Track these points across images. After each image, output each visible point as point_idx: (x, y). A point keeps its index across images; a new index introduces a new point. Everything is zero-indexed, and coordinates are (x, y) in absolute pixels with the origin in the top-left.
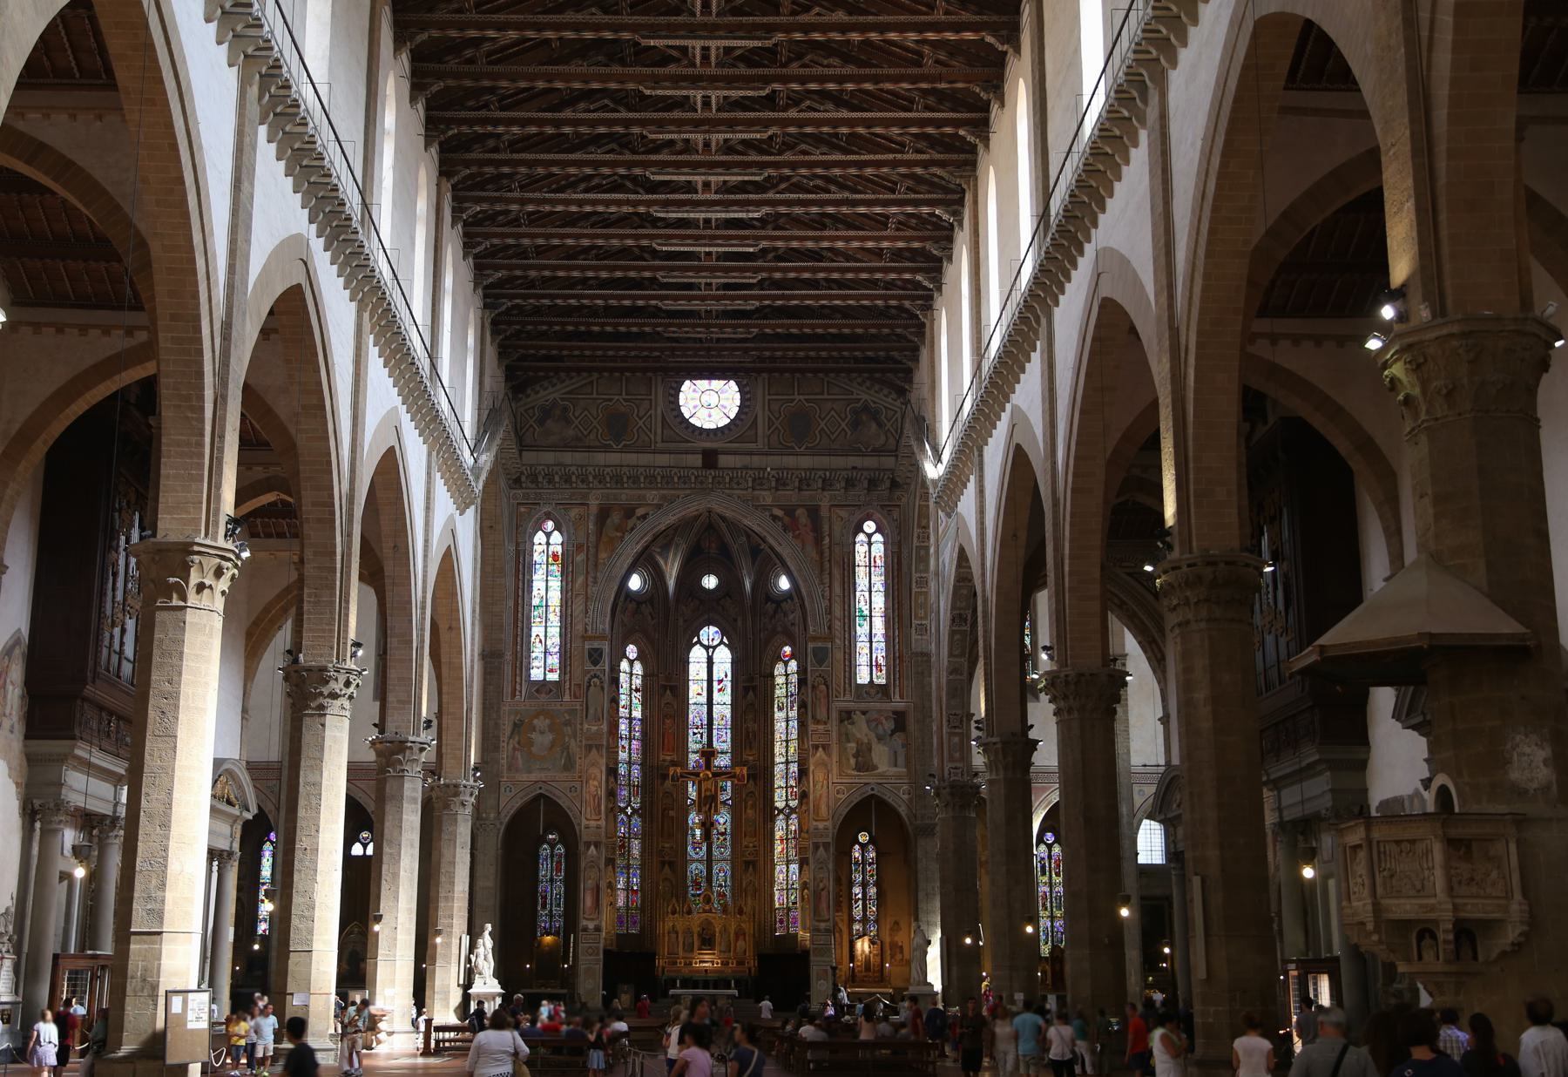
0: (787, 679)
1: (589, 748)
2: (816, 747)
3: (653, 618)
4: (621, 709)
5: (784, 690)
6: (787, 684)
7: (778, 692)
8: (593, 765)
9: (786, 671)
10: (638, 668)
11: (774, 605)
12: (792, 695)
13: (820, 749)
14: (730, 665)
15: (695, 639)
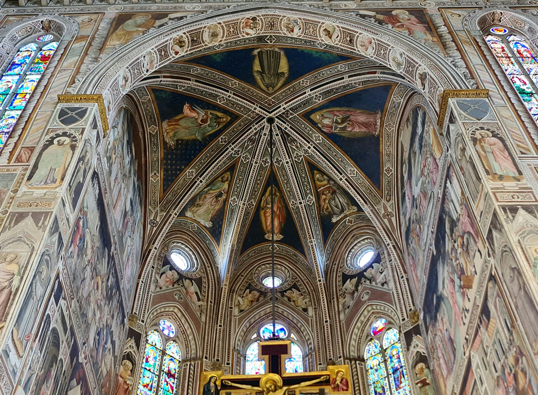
0: (384, 356)
1: (21, 216)
2: (514, 210)
3: (199, 300)
4: (141, 387)
5: (383, 372)
6: (385, 361)
7: (372, 377)
8: (19, 239)
9: (381, 347)
10: (174, 350)
11: (355, 280)
12: (395, 371)
13: (521, 212)
14: (301, 364)
15: (255, 336)
